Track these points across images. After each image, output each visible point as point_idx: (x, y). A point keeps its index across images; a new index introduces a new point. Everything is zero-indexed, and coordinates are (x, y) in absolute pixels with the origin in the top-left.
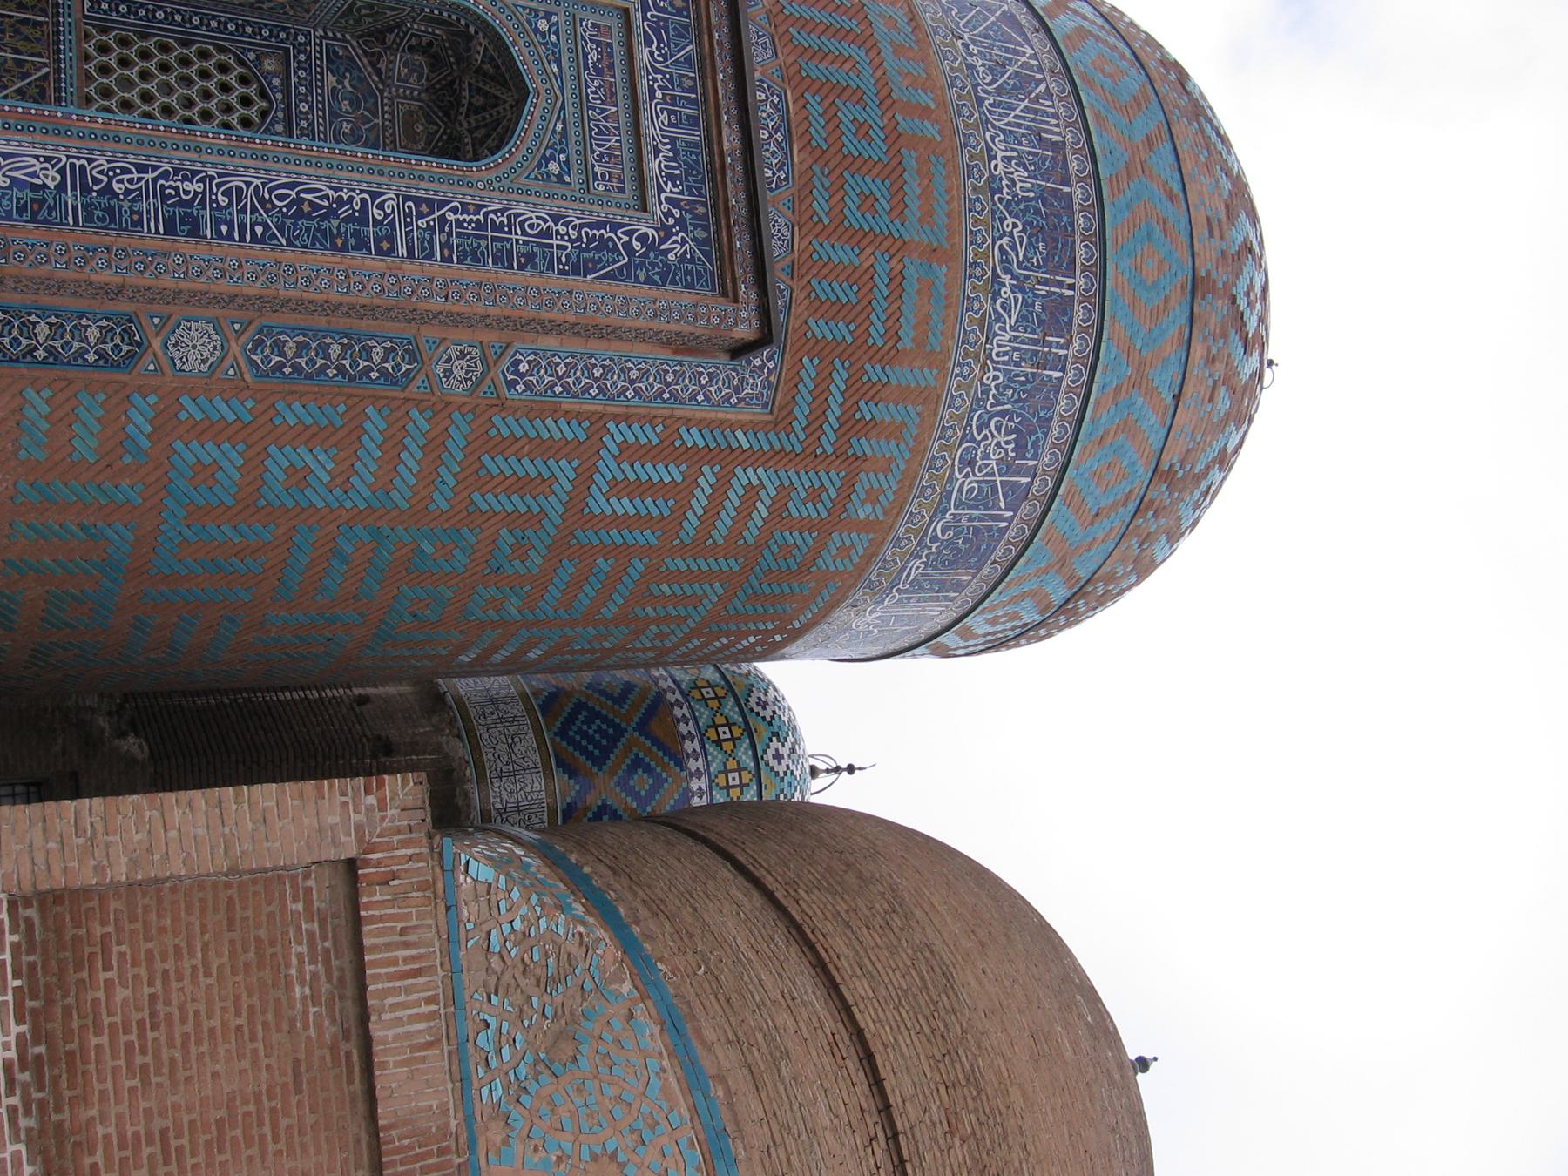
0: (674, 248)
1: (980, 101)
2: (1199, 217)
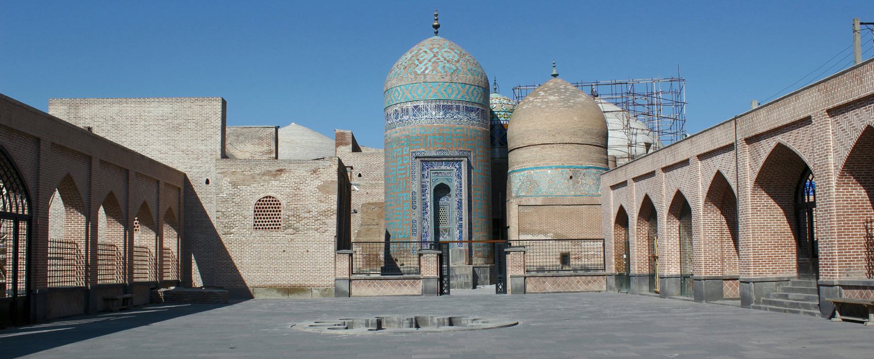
0: (457, 167)
1: (431, 119)
2: (442, 80)
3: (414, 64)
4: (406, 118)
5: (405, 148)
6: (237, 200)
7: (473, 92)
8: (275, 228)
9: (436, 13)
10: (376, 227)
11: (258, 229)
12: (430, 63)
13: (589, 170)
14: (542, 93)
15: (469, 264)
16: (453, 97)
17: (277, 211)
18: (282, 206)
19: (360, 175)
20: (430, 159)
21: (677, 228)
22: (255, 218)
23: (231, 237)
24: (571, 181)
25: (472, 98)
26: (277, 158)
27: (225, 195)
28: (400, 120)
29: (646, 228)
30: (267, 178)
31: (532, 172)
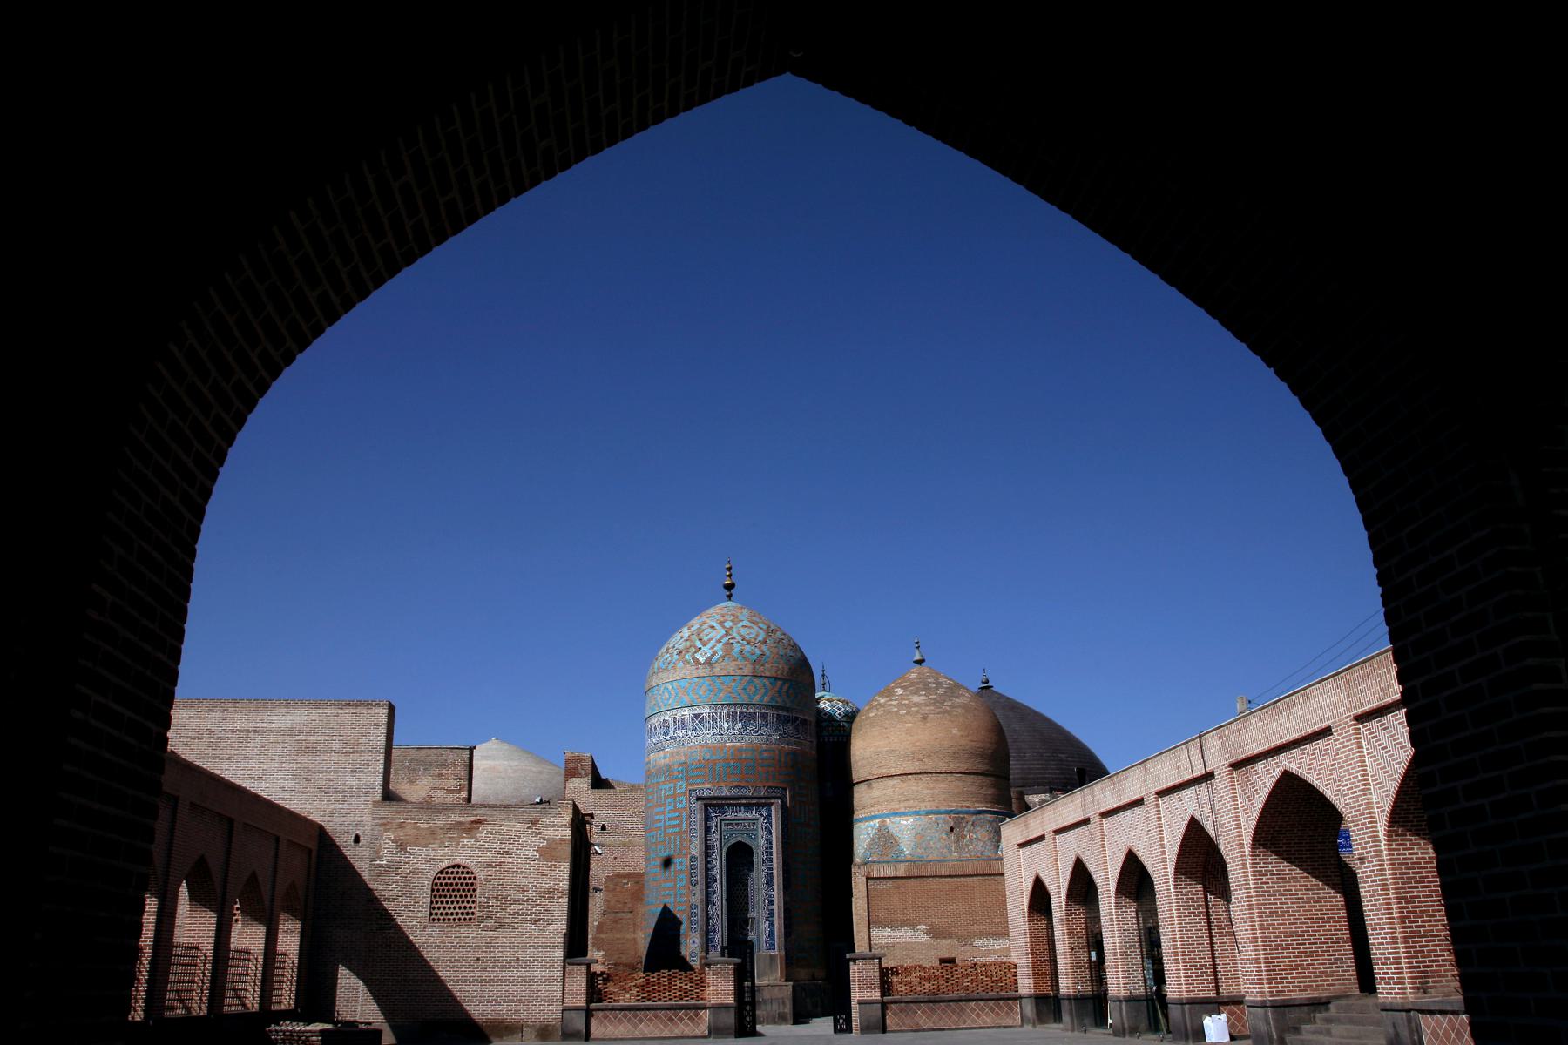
0: (765, 814)
2: (739, 672)
3: (695, 647)
4: (680, 733)
5: (679, 784)
6: (405, 870)
7: (787, 692)
8: (465, 919)
9: (728, 566)
10: (630, 915)
11: (436, 921)
12: (719, 646)
13: (981, 816)
14: (900, 691)
15: (786, 981)
16: (756, 699)
17: (469, 890)
18: (478, 881)
19: (603, 828)
20: (720, 802)
21: (1134, 914)
22: (432, 902)
23: (392, 935)
24: (953, 837)
25: (787, 701)
26: (469, 799)
27: (385, 862)
28: (672, 738)
29: (1080, 915)
30: (455, 834)
31: (888, 821)
